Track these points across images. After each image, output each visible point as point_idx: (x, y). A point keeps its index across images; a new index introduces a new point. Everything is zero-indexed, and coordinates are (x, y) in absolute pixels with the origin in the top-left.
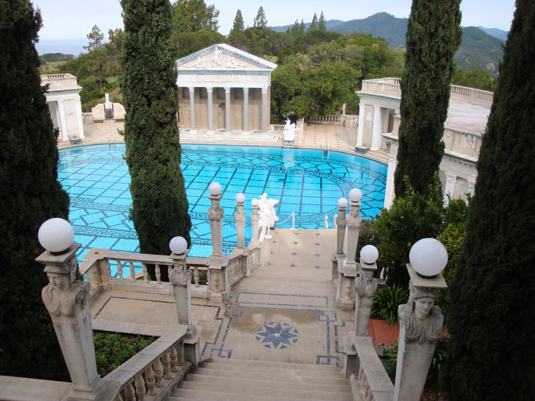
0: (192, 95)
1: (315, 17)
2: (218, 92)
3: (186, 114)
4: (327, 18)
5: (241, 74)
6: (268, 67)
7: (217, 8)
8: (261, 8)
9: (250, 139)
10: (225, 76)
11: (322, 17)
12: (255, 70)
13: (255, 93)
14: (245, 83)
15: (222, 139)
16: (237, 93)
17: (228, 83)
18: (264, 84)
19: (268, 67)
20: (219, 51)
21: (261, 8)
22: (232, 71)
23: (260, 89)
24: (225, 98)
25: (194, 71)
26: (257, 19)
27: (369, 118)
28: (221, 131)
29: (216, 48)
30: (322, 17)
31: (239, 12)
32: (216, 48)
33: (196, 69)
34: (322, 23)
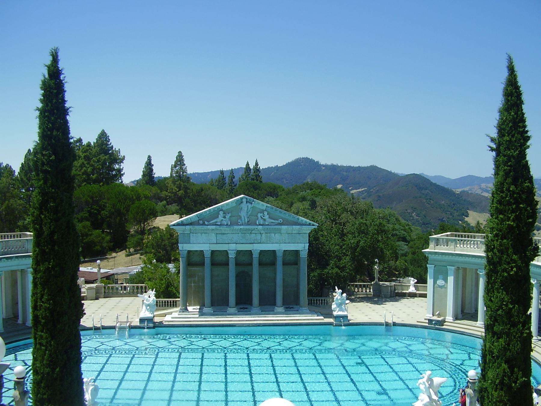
0: (208, 262)
1: (248, 164)
4: (262, 166)
5: (275, 234)
6: (310, 224)
7: (122, 154)
8: (180, 152)
10: (253, 235)
11: (257, 164)
20: (248, 204)
21: (180, 152)
23: (297, 252)
24: (251, 264)
25: (213, 230)
26: (175, 167)
28: (241, 308)
29: (244, 200)
30: (257, 164)
31: (149, 157)
32: (244, 200)
34: (257, 169)
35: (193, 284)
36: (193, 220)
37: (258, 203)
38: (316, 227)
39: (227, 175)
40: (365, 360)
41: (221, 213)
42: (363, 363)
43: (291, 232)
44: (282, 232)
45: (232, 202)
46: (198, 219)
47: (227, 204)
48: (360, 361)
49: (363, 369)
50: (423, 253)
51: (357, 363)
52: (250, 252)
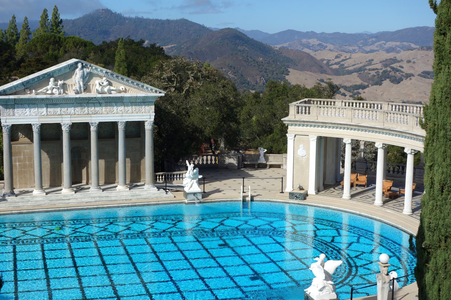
2: (80, 131)
3: (16, 165)
9: (133, 196)
11: (56, 16)
12: (139, 95)
13: (135, 130)
14: (121, 116)
15: (90, 200)
16: (108, 131)
17: (95, 117)
18: (147, 115)
19: (156, 92)
22: (103, 98)
25: (42, 99)
29: (80, 65)
30: (56, 16)
33: (49, 96)
35: (17, 163)
36: (18, 89)
37: (96, 69)
38: (163, 95)
39: (20, 29)
40: (228, 241)
41: (52, 80)
42: (225, 245)
43: (134, 101)
44: (124, 101)
45: (65, 67)
46: (24, 88)
47: (60, 70)
48: (221, 242)
49: (227, 251)
50: (282, 121)
51: (220, 245)
52: (86, 126)
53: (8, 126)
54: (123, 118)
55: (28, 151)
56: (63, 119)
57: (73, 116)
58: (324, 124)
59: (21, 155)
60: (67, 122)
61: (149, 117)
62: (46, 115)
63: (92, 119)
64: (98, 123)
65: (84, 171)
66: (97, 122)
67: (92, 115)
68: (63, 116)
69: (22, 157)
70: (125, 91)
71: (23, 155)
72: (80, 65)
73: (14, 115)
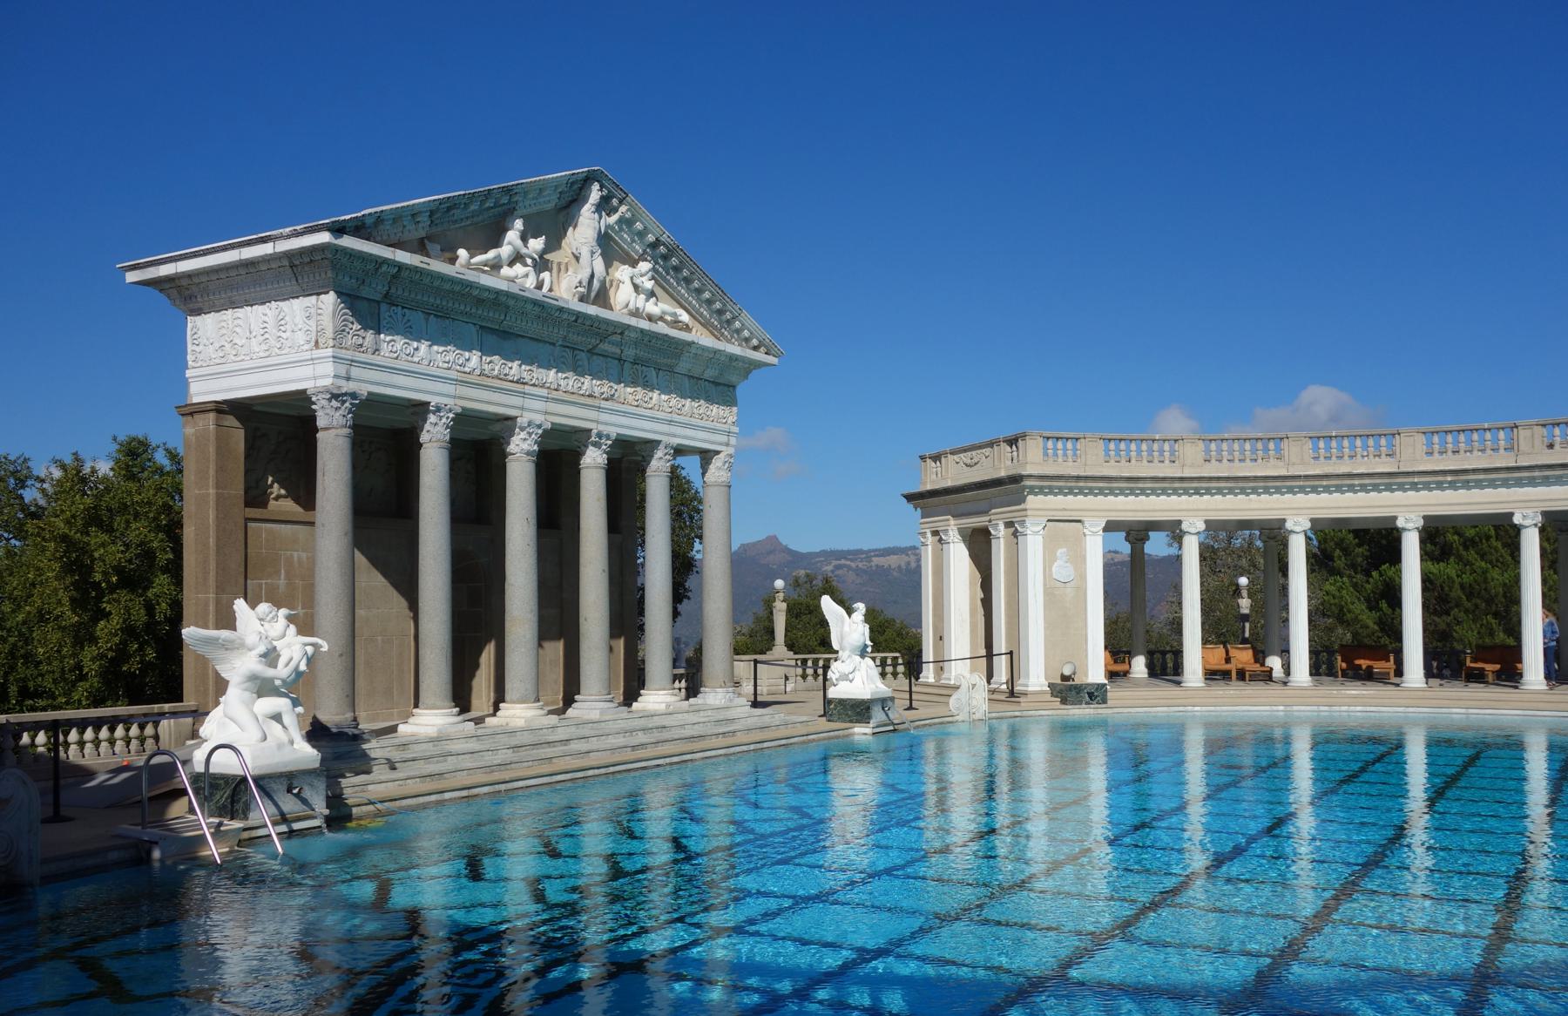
27: (1062, 570)
46: (423, 234)
53: (353, 395)
54: (673, 429)
55: (304, 555)
56: (529, 403)
57: (555, 394)
58: (1133, 485)
59: (278, 573)
60: (538, 418)
61: (724, 439)
62: (478, 372)
63: (604, 417)
64: (614, 436)
65: (487, 657)
66: (613, 432)
67: (604, 404)
68: (528, 389)
69: (282, 582)
70: (687, 328)
71: (288, 577)
72: (595, 194)
73: (376, 351)
